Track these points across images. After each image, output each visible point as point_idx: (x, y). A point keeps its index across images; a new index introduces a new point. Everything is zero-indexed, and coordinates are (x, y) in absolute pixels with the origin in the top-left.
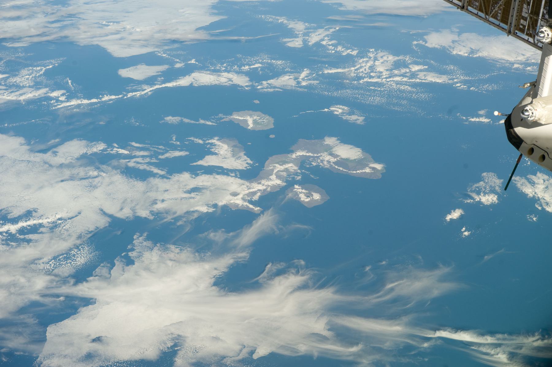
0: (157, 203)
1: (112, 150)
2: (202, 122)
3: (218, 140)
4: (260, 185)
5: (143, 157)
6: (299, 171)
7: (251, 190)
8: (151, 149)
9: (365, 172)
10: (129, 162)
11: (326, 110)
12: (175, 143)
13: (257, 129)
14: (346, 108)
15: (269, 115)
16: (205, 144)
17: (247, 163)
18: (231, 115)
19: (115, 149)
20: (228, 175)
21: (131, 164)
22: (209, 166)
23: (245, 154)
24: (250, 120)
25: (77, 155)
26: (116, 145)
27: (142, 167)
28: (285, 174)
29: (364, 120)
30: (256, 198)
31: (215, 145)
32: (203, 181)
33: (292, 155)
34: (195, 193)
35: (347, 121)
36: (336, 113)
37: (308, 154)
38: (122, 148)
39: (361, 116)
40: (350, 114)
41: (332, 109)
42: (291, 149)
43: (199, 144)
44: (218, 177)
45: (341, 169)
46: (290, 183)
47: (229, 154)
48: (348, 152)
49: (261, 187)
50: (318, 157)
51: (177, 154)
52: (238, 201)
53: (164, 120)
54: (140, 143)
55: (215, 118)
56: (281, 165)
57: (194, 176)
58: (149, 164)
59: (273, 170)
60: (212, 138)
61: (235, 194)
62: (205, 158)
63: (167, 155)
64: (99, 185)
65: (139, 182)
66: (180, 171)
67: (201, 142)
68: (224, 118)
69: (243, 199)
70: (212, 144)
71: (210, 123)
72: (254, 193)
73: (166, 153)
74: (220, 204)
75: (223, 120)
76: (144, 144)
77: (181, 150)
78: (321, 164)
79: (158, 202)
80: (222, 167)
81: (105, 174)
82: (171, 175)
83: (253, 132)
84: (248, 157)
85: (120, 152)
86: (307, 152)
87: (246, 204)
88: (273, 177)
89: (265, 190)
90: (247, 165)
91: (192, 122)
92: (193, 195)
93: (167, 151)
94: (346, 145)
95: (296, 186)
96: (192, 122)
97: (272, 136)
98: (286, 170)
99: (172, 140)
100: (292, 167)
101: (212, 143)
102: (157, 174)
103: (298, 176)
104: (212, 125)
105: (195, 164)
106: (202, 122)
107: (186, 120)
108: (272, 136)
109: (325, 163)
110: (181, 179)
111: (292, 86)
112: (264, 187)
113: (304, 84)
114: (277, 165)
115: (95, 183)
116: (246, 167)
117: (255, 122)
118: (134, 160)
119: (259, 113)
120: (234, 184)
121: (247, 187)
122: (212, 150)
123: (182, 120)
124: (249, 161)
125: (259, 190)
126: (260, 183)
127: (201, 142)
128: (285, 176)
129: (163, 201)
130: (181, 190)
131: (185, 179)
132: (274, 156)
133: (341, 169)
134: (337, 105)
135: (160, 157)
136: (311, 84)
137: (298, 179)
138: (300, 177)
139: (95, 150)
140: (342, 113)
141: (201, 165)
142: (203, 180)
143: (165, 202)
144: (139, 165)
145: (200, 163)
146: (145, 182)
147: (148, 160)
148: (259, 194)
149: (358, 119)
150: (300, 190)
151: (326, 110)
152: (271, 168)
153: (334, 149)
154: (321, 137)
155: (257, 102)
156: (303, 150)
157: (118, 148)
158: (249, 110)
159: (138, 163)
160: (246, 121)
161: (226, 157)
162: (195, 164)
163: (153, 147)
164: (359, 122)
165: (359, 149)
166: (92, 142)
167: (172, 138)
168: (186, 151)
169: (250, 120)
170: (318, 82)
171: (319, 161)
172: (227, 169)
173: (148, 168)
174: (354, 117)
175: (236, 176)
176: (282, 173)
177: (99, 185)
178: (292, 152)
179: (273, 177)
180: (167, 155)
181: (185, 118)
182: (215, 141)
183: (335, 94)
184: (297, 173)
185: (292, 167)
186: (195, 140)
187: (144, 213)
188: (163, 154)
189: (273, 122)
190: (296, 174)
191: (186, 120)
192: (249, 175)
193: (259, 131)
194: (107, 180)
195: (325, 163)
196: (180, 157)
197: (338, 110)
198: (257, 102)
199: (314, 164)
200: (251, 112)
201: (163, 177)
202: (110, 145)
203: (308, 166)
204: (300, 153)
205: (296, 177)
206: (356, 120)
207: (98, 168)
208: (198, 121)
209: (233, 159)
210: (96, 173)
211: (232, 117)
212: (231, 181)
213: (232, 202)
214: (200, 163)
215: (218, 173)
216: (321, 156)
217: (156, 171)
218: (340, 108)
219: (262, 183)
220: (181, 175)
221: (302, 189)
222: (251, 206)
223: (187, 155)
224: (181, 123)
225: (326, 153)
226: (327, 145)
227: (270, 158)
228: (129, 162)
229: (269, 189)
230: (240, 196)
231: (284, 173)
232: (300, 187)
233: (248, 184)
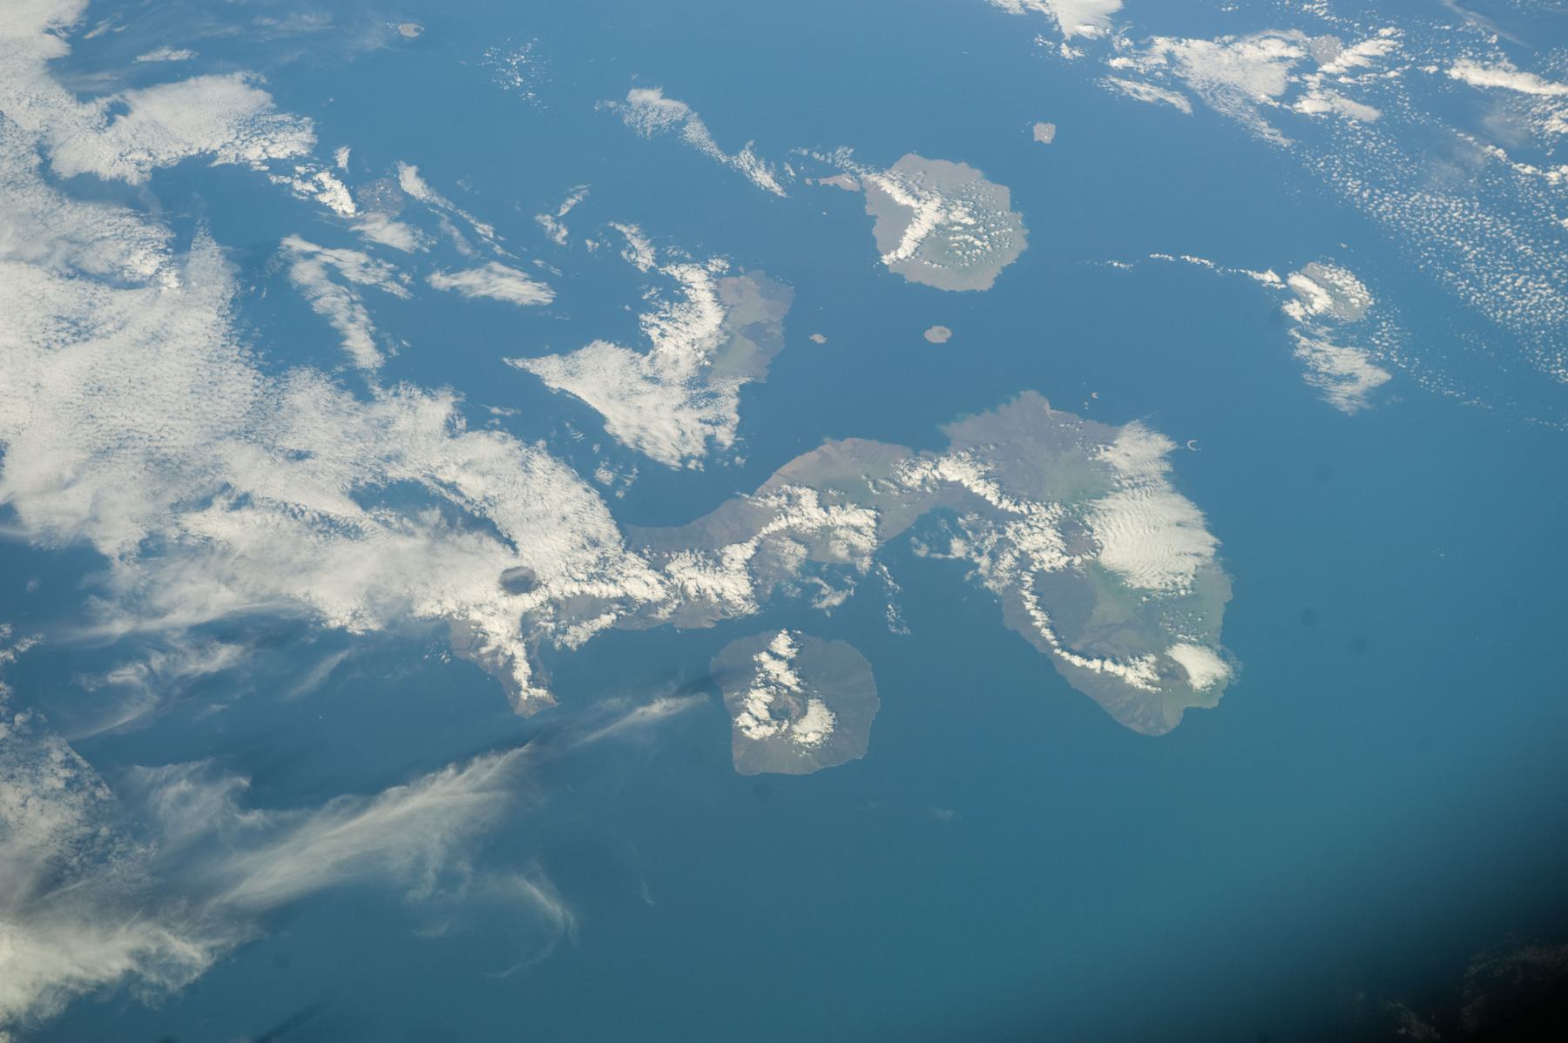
0: (205, 504)
1: (305, 178)
2: (745, 159)
3: (716, 277)
4: (652, 577)
5: (380, 252)
6: (866, 563)
7: (598, 589)
8: (444, 225)
9: (1120, 679)
10: (309, 256)
11: (1270, 277)
12: (550, 226)
13: (912, 277)
14: (1358, 294)
15: (1027, 221)
16: (654, 277)
17: (709, 440)
18: (882, 166)
19: (324, 177)
20: (585, 472)
21: (305, 273)
22: (563, 392)
23: (743, 392)
24: (927, 219)
25: (170, 153)
26: (343, 157)
27: (330, 300)
28: (794, 554)
29: (1375, 394)
30: (579, 634)
31: (683, 298)
32: (465, 467)
33: (912, 467)
34: (389, 515)
35: (1302, 365)
36: (1294, 310)
37: (979, 488)
38: (346, 183)
39: (1380, 364)
40: (1347, 333)
41: (1298, 281)
42: (949, 429)
43: (632, 267)
44: (541, 463)
45: (1040, 618)
46: (780, 606)
47: (686, 368)
48: (1149, 538)
49: (641, 584)
50: (1002, 518)
51: (514, 287)
52: (501, 626)
53: (622, 97)
54: (429, 183)
55: (809, 158)
56: (823, 504)
57: (461, 424)
58: (371, 298)
59: (770, 516)
60: (700, 259)
61: (518, 583)
62: (587, 351)
63: (472, 281)
64: (110, 327)
65: (250, 373)
66: (429, 383)
67: (645, 258)
68: (840, 171)
69: (527, 623)
70: (675, 293)
71: (764, 178)
72: (595, 607)
73: (474, 265)
74: (427, 608)
75: (830, 182)
76: (441, 192)
77: (535, 275)
78: (984, 561)
79: (220, 502)
80: (602, 419)
81: (174, 284)
82: (386, 386)
83: (893, 281)
84: (740, 410)
85: (324, 199)
86: (987, 477)
87: (518, 650)
88: (739, 553)
89: (650, 606)
90: (698, 448)
91: (711, 148)
92: (366, 520)
93: (482, 257)
94: (1177, 499)
95: (782, 643)
96: (711, 148)
97: (937, 335)
98: (827, 531)
99: (553, 209)
100: (855, 526)
101: (678, 285)
102: (347, 357)
103: (838, 586)
104: (768, 192)
105: (520, 363)
106: (745, 159)
107: (695, 132)
108: (937, 335)
109: (1007, 560)
110: (404, 423)
111: (1250, 101)
112: (659, 593)
113: (1309, 106)
114: (808, 498)
115: (100, 314)
116: (684, 460)
117: (937, 241)
118: (330, 256)
119: (1000, 194)
120: (558, 532)
121: (603, 560)
122: (650, 318)
123: (684, 122)
124: (725, 436)
125: (626, 601)
126: (657, 566)
127: (645, 258)
128: (791, 565)
129: (243, 502)
130: (350, 473)
131: (423, 432)
132: (847, 444)
133: (1040, 618)
134: (1338, 265)
135: (440, 281)
136: (1333, 116)
137: (824, 604)
138: (837, 601)
139: (254, 153)
140: (1323, 319)
141: (537, 380)
142: (481, 464)
143: (247, 514)
144: (329, 287)
145: (551, 371)
146: (271, 381)
147: (375, 276)
148: (606, 620)
149: (1352, 372)
150: (776, 668)
151: (1270, 277)
152: (773, 502)
153: (1108, 503)
154: (1112, 417)
155: (1044, 133)
156: (978, 458)
157: (337, 174)
158: (973, 163)
159: (334, 274)
160: (907, 216)
161: (667, 375)
162: (520, 363)
163: (456, 221)
164: (1341, 396)
165: (1205, 543)
166: (281, 109)
167: (562, 200)
168: (553, 283)
169: (927, 219)
170: (1370, 113)
171: (994, 537)
172: (609, 442)
173: (341, 319)
174: (1348, 360)
175: (606, 494)
176: (789, 546)
177: (110, 327)
178: (937, 447)
179: (739, 553)
180: (472, 281)
181: (701, 117)
182: (696, 280)
183: (1386, 206)
184: (850, 568)
185: (855, 526)
186: (636, 243)
187: (117, 536)
188: (457, 264)
189: (1011, 258)
190: (837, 573)
191: (695, 132)
192: (658, 505)
193: (919, 287)
194: (152, 318)
195: (1007, 560)
196: (507, 305)
197: (1317, 292)
198: (1044, 133)
199: (958, 548)
200: (968, 176)
201: (356, 385)
202: (321, 156)
203: (922, 552)
204: (954, 470)
205: (826, 589)
206: (1340, 379)
207: (178, 248)
208: (732, 149)
209: (678, 395)
210: (148, 269)
211: (873, 178)
212: (567, 509)
213: (476, 616)
214: (551, 371)
215: (557, 451)
216: (1022, 517)
217: (362, 348)
218: (1331, 289)
219: (672, 567)
220: (426, 401)
221: (791, 664)
222: (522, 672)
223: (537, 307)
224: (670, 136)
225: (1057, 509)
226: (1107, 467)
227: (828, 447)
228: (309, 256)
229: (663, 614)
230: (527, 602)
231: (801, 551)
232: (791, 653)
233: (613, 549)
